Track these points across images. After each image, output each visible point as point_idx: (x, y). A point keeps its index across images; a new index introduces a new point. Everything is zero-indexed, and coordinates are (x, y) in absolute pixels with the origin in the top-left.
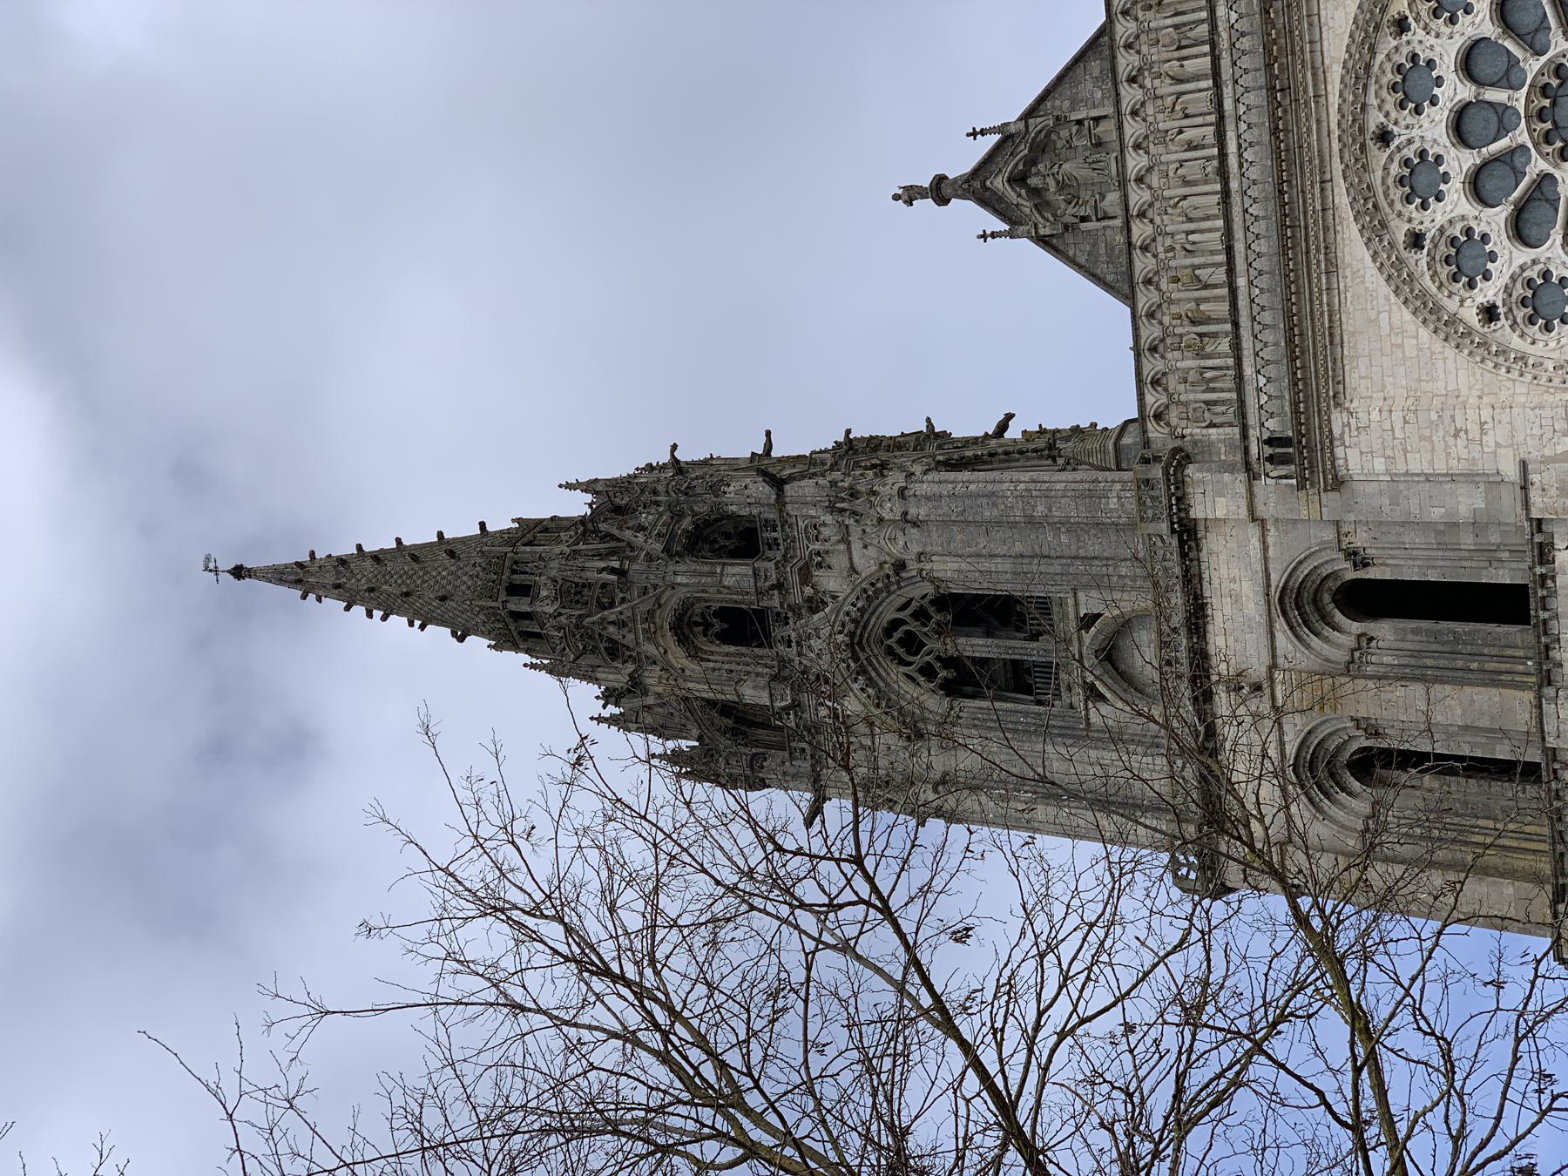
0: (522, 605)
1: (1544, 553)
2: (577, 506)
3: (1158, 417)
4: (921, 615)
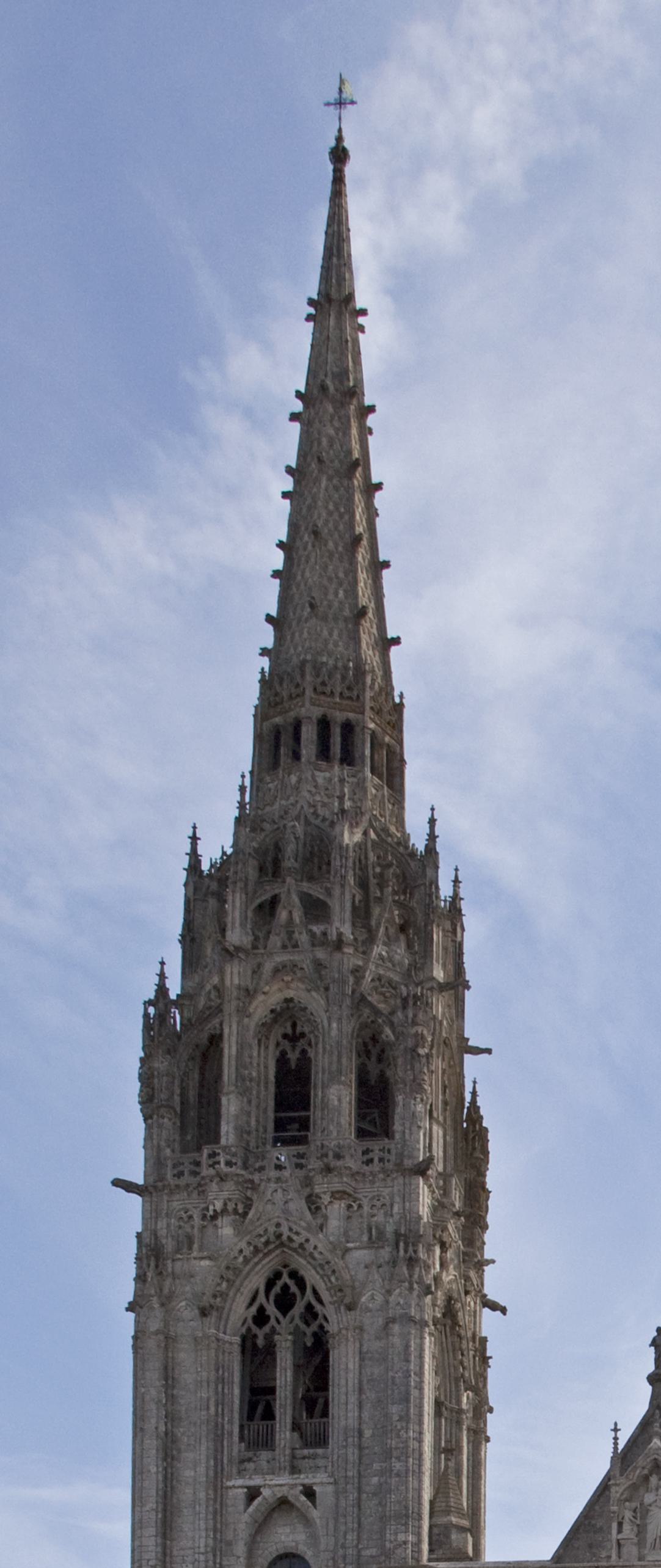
4: (310, 1313)
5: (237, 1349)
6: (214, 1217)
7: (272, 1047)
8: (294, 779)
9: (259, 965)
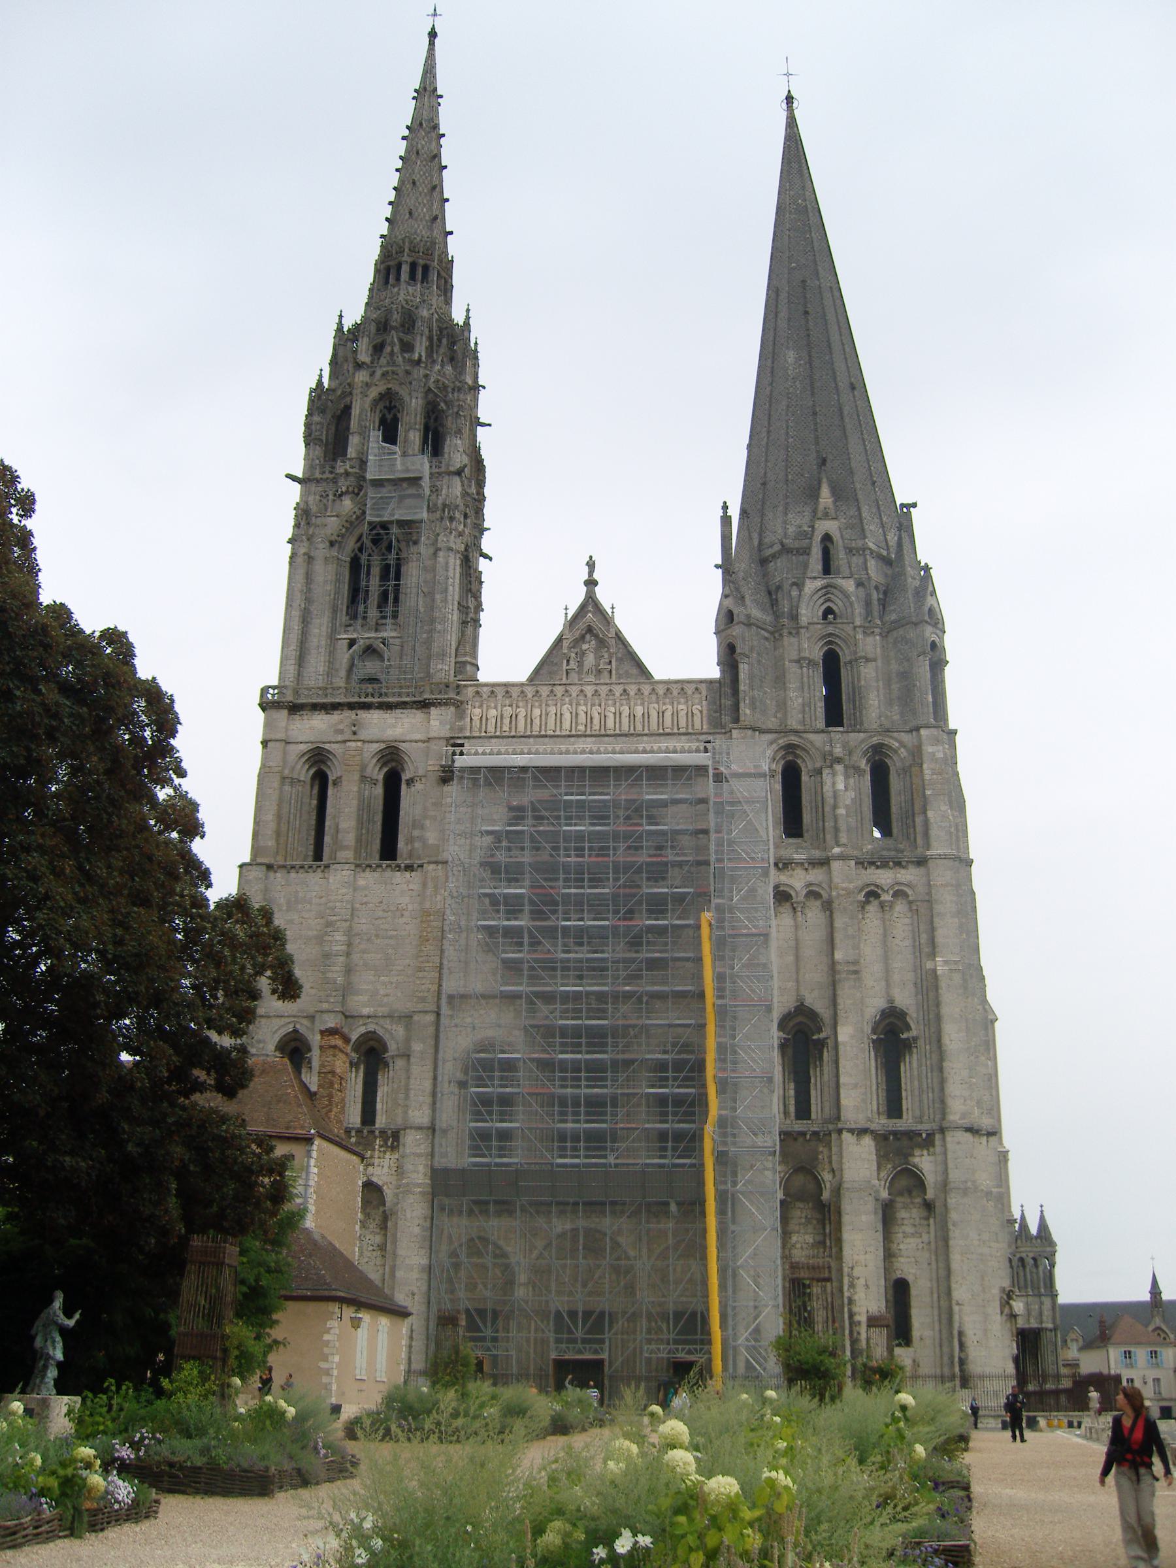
0: (405, 276)
1: (409, 868)
2: (458, 317)
3: (478, 693)
5: (348, 565)
6: (340, 496)
7: (378, 411)
8: (396, 289)
9: (374, 372)
